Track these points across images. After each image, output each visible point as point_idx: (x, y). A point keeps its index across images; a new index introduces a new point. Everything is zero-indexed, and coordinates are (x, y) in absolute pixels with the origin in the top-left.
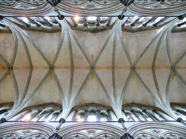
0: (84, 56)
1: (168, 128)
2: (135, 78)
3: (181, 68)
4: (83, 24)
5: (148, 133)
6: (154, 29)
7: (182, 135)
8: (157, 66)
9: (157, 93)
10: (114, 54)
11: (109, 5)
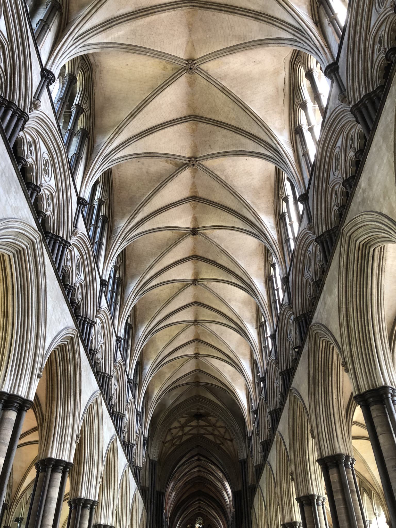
1: (60, 188)
2: (163, 71)
3: (194, 177)
5: (39, 154)
6: (290, 125)
7: (56, 217)
8: (197, 127)
9: (129, 137)
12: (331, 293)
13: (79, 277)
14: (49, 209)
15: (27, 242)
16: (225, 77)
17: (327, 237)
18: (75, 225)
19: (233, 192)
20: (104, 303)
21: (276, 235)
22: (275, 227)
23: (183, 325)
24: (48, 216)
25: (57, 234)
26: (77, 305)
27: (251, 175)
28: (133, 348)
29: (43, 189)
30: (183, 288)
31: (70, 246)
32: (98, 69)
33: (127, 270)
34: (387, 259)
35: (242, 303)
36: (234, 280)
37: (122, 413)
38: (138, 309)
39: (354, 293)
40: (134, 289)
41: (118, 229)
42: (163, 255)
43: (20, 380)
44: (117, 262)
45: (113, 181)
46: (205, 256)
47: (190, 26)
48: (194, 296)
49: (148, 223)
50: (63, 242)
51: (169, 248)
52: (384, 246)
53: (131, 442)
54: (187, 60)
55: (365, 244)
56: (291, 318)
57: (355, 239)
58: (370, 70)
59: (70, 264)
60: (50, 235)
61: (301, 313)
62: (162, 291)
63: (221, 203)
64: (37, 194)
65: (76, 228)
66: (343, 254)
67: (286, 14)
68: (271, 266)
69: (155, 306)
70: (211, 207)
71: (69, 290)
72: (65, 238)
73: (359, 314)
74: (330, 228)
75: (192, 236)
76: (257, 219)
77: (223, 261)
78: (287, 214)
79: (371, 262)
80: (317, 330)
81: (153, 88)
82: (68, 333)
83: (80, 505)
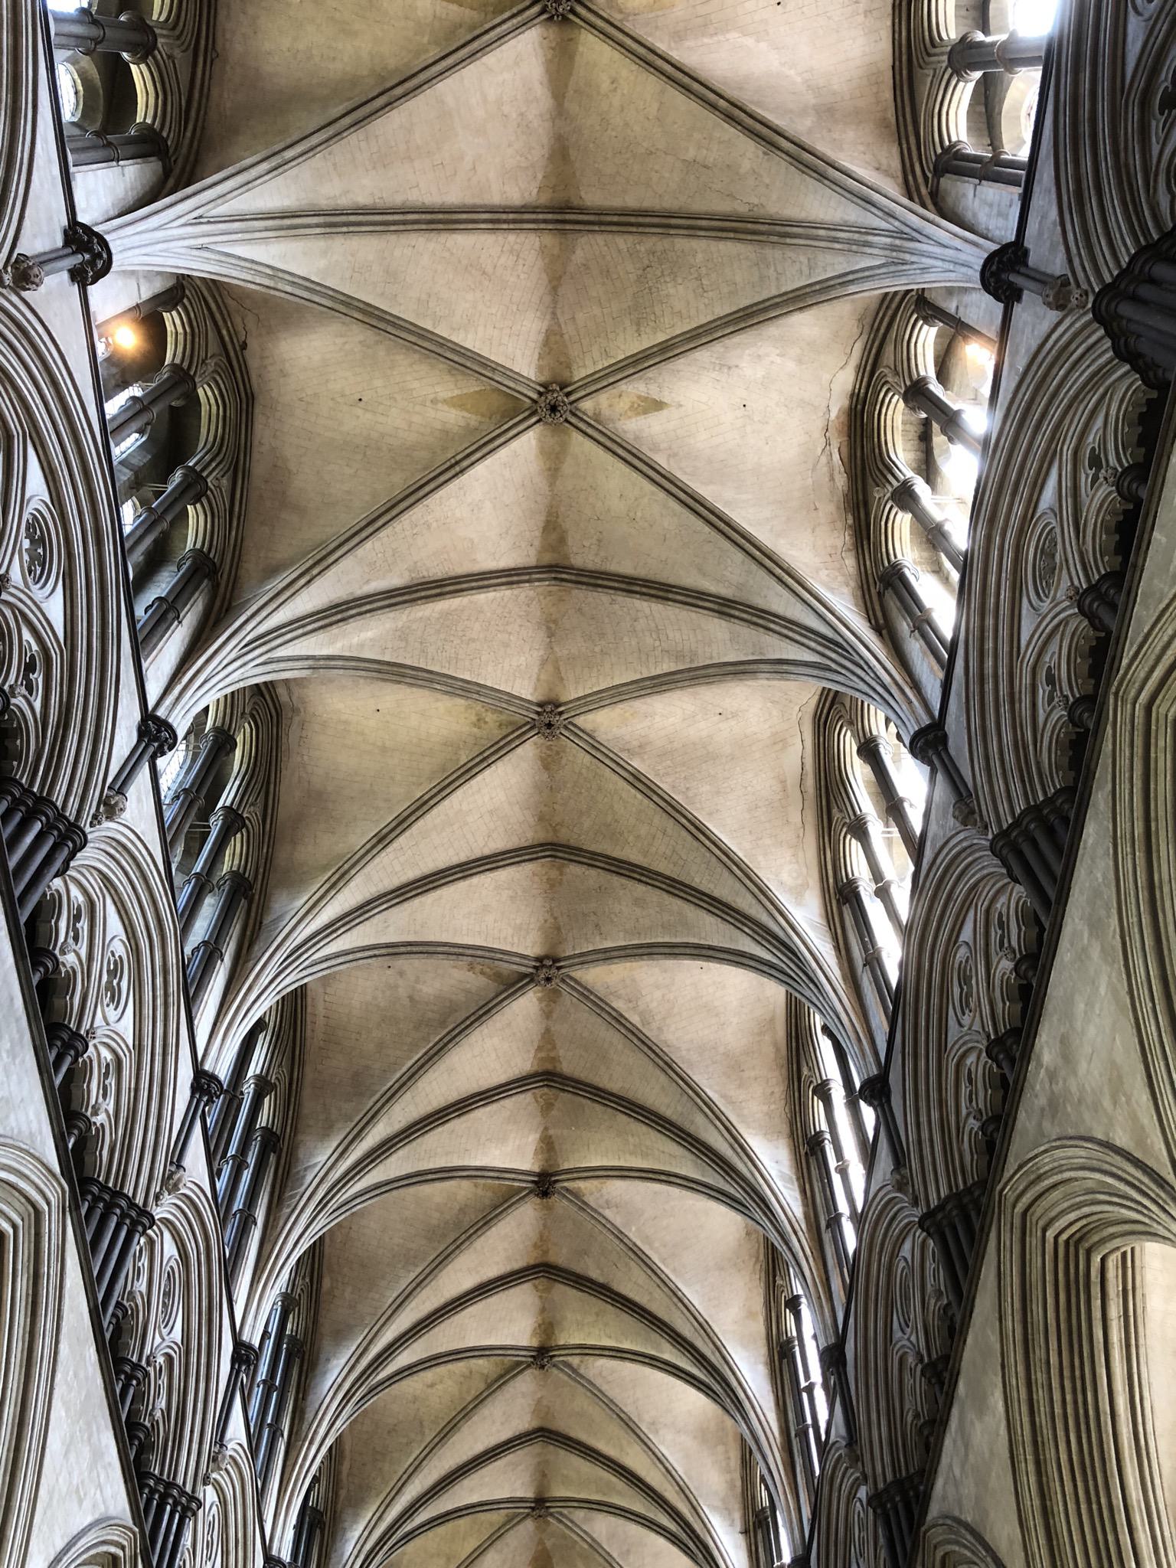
0: (661, 337)
1: (147, 1042)
2: (475, 730)
3: (547, 1014)
4: (963, 136)
5: (98, 941)
9: (368, 897)
10: (660, 591)
11: (951, 1103)
12: (982, 1407)
13: (165, 1332)
14: (104, 1106)
15: (20, 1214)
16: (642, 748)
17: (954, 1213)
18: (177, 1161)
19: (666, 1063)
20: (236, 1430)
21: (800, 1203)
22: (794, 1177)
23: (497, 1517)
24: (97, 1129)
25: (115, 1185)
26: (148, 1435)
27: (717, 1015)
29: (95, 1046)
30: (501, 1376)
31: (150, 1227)
32: (296, 719)
33: (323, 1312)
34: (1147, 1291)
35: (695, 1437)
36: (669, 1354)
38: (347, 1453)
39: (1058, 1410)
40: (339, 1380)
41: (308, 1173)
42: (443, 1260)
44: (292, 1283)
45: (308, 1023)
46: (578, 1268)
47: (553, 626)
48: (539, 1408)
49: (401, 1153)
50: (133, 1214)
51: (464, 1237)
52: (1133, 1249)
54: (540, 705)
55: (1072, 1242)
56: (858, 1495)
57: (1041, 1223)
58: (1031, 748)
59: (144, 1288)
60: (95, 1190)
61: (890, 1477)
62: (432, 1386)
63: (630, 1095)
64: (75, 1061)
65: (179, 1166)
66: (1008, 1272)
67: (799, 606)
68: (786, 1307)
69: (405, 1440)
70: (598, 1107)
71: (130, 1377)
72: (139, 1200)
73: (1080, 1484)
74: (961, 1187)
75: (538, 1200)
76: (739, 1150)
77: (633, 1285)
78: (828, 1136)
79: (1099, 1302)
80: (949, 1542)
81: (444, 770)
82: (104, 1543)
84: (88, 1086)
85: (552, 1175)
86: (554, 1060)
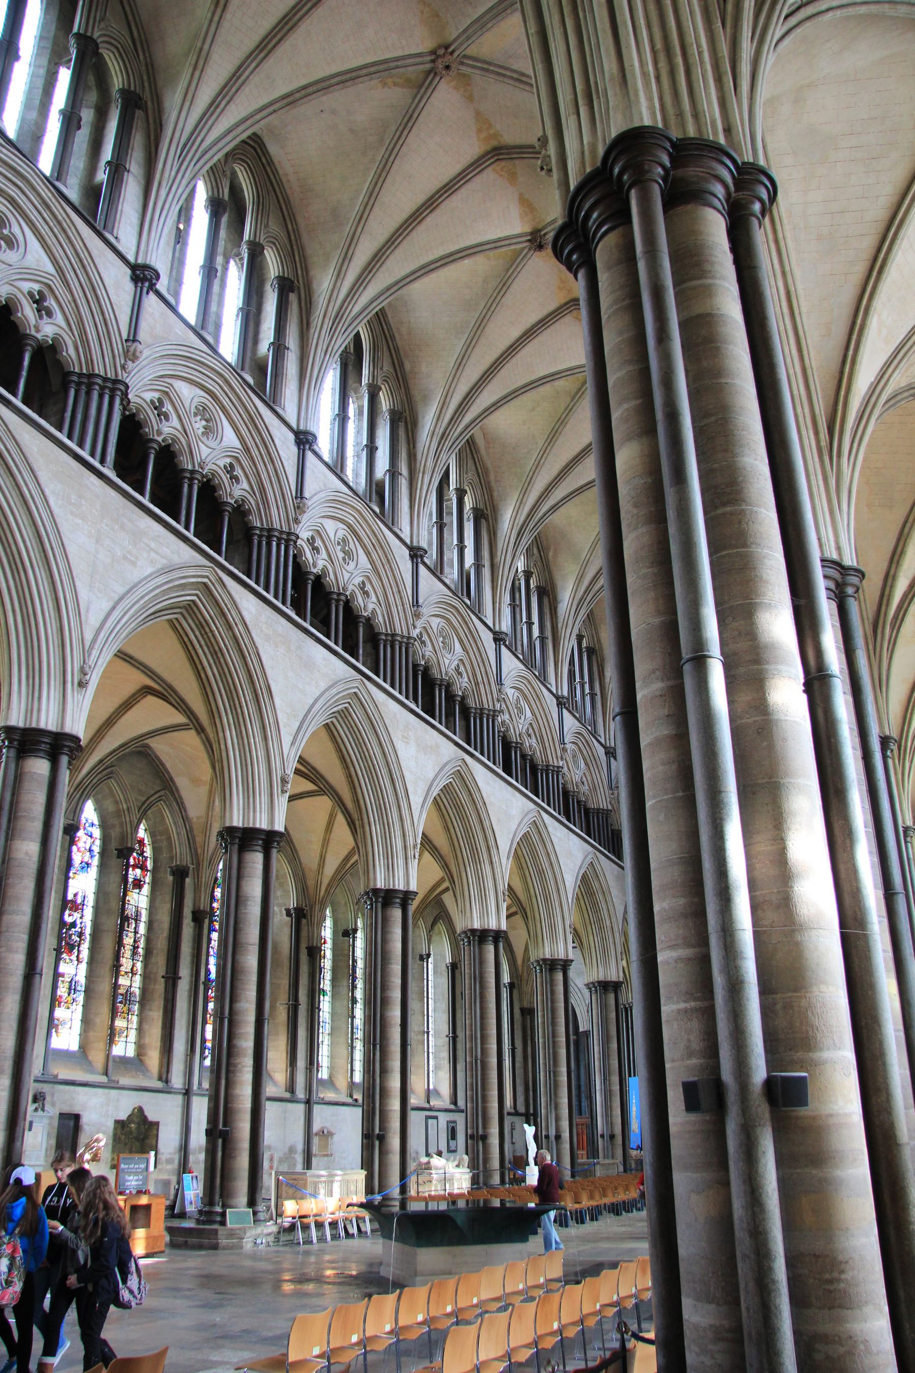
3: (470, 98)
28: (495, 561)
37: (491, 708)
38: (490, 469)
42: (480, 325)
43: (40, 698)
50: (109, 385)
53: (551, 763)
75: (537, 253)
83: (376, 902)
84: (22, 314)
85: (540, 231)
86: (495, 136)
